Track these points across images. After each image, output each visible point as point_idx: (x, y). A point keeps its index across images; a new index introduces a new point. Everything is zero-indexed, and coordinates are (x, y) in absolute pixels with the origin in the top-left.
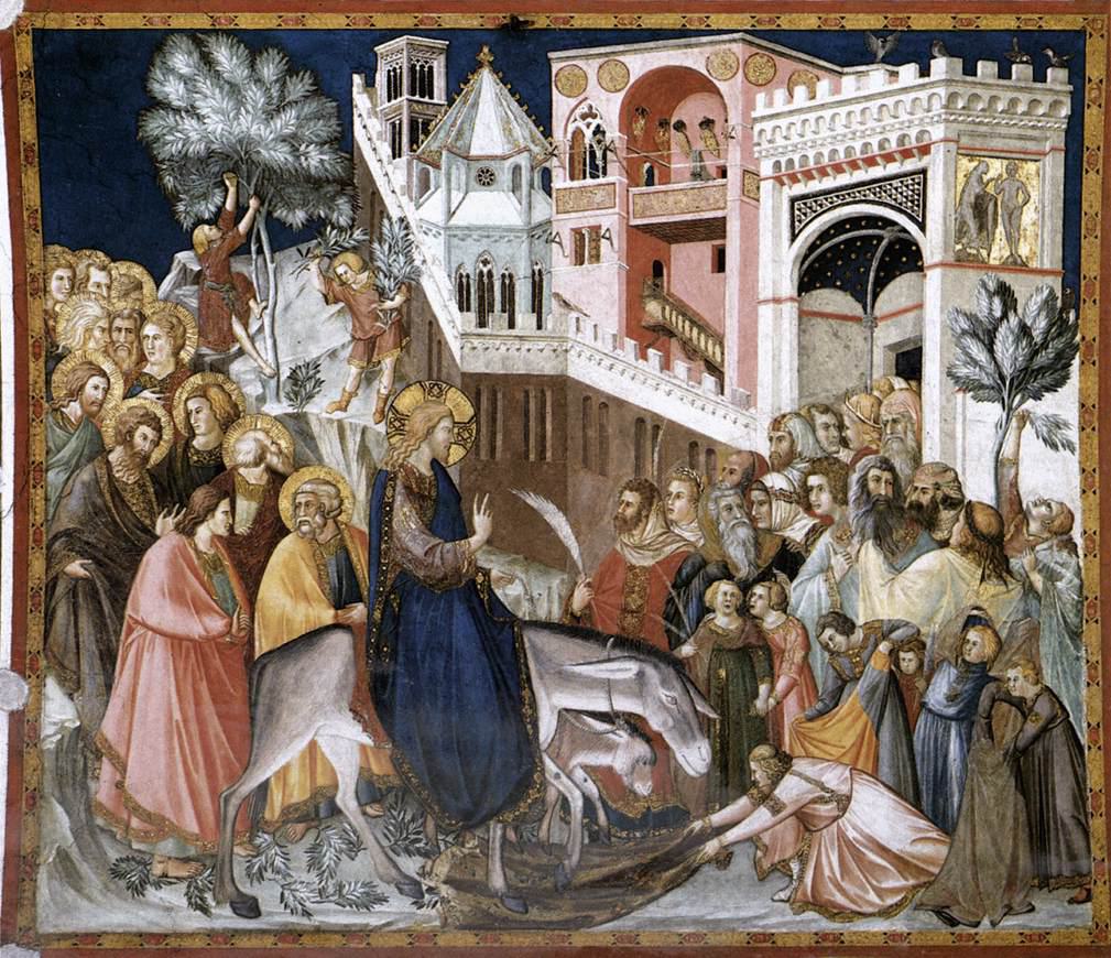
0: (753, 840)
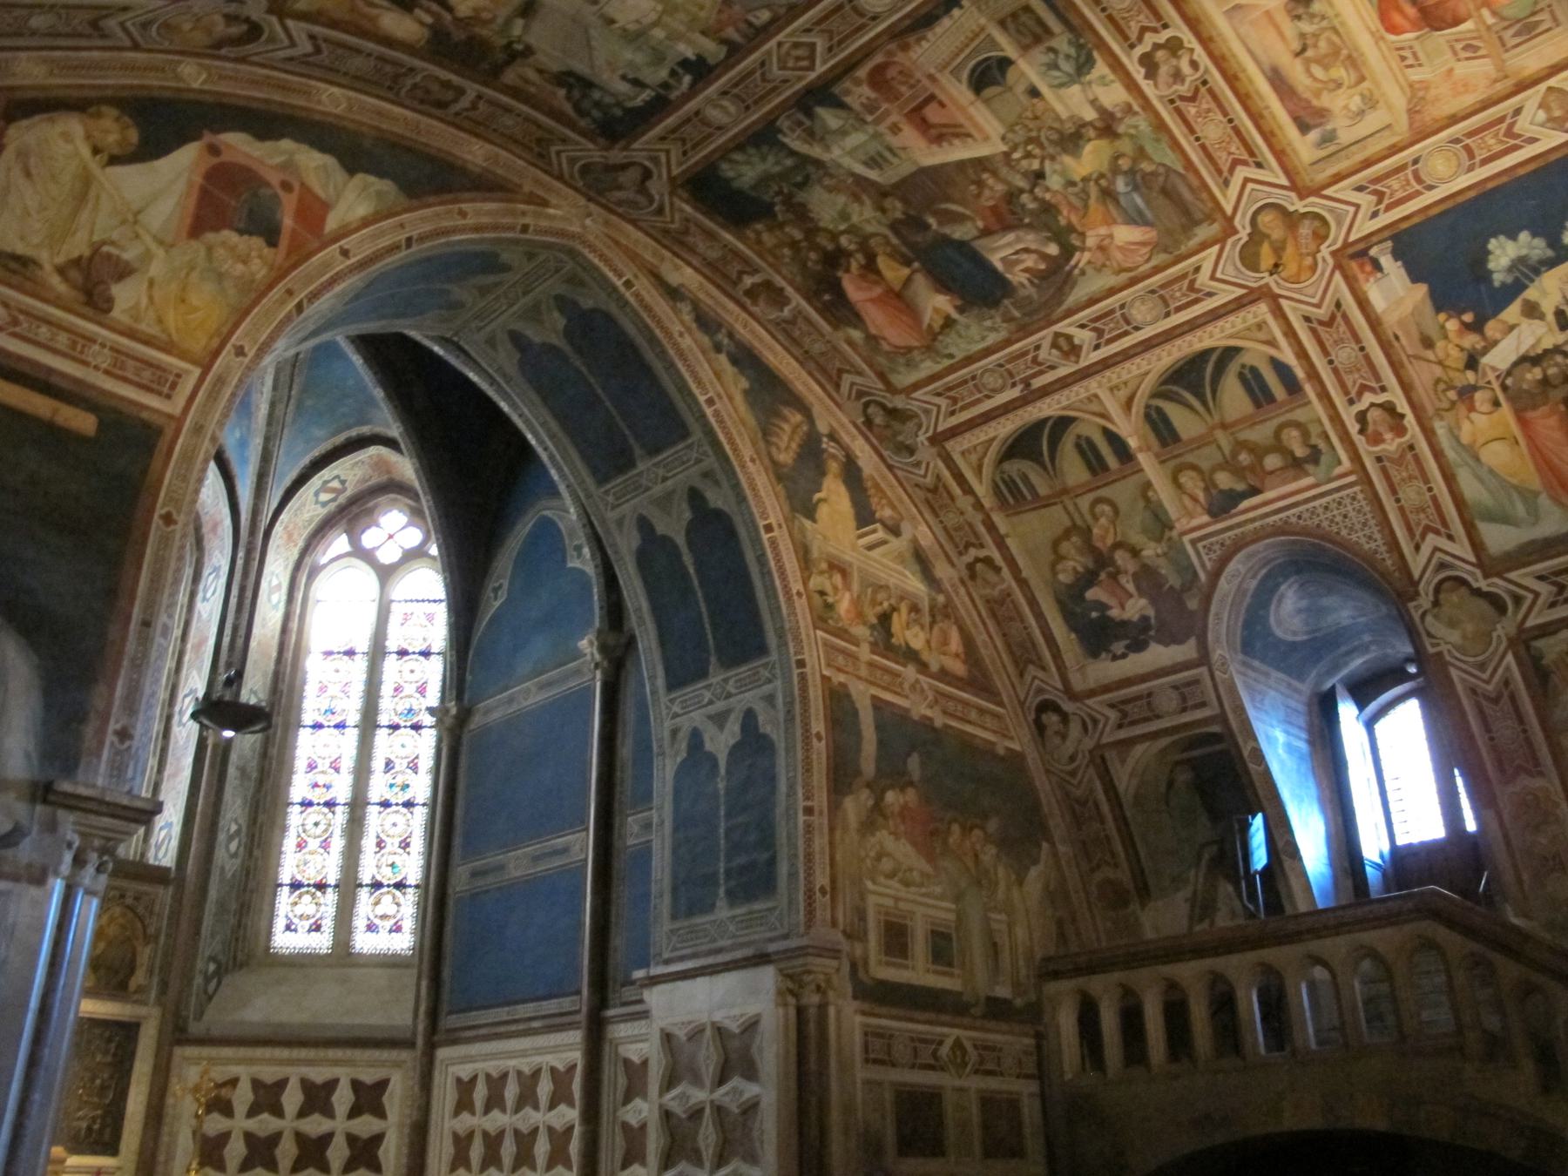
0: (1089, 262)
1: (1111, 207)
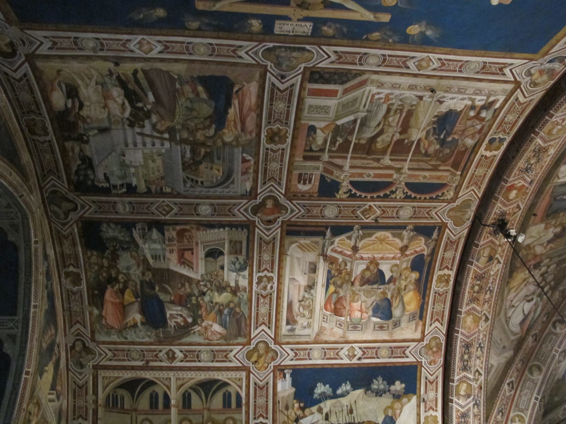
0: (199, 331)
1: (218, 317)
